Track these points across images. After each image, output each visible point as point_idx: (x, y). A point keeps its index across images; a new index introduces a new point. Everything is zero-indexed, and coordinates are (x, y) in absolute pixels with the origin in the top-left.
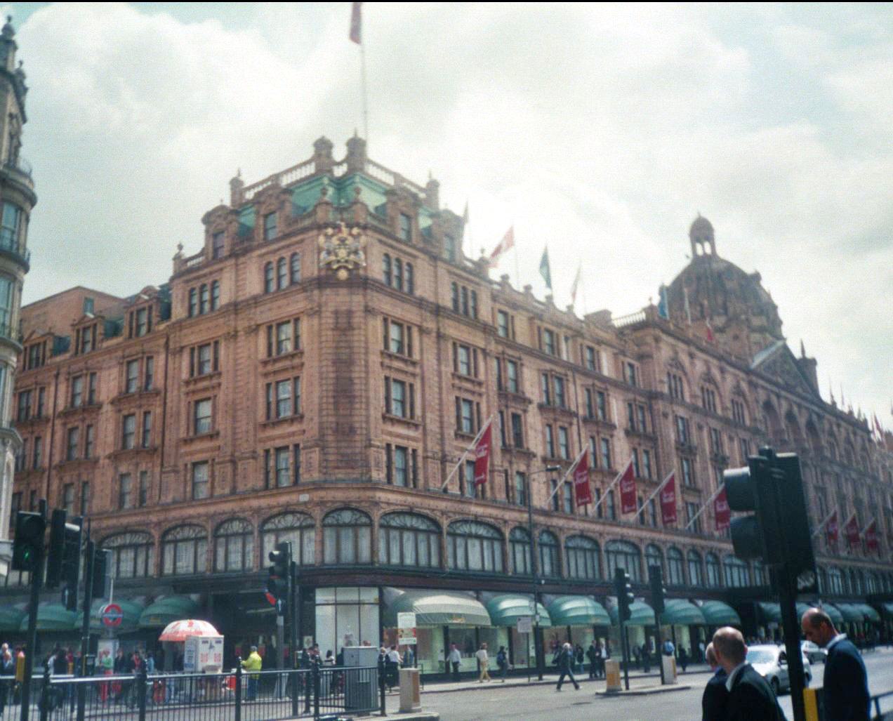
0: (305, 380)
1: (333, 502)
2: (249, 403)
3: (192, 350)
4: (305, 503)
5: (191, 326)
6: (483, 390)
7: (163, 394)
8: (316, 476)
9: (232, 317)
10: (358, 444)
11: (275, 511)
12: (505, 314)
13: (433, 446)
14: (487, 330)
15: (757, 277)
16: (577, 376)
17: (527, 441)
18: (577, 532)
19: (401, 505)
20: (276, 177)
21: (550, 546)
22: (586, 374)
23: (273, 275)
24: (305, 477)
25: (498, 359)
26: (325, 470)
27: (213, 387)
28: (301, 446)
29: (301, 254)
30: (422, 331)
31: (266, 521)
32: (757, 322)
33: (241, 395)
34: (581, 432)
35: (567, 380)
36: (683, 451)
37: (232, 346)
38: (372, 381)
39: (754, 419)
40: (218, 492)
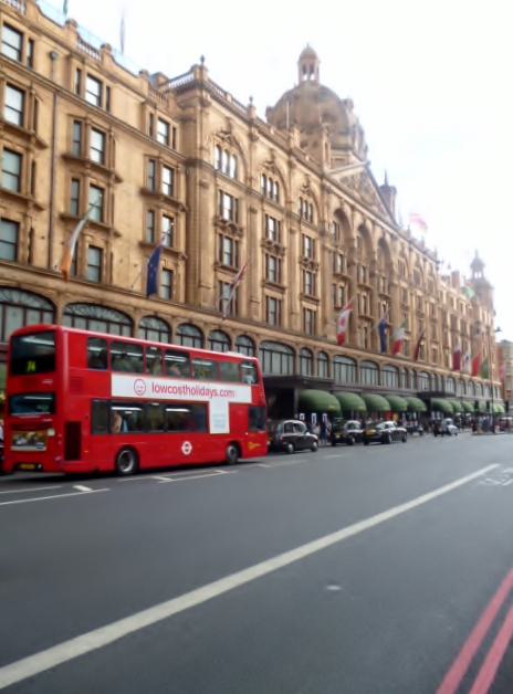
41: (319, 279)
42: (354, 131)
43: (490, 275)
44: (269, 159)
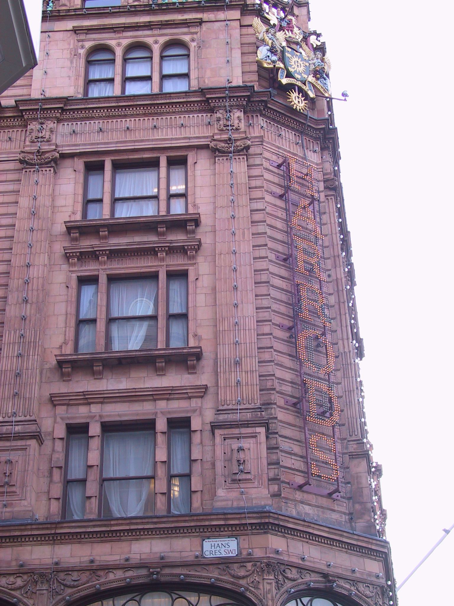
0: (205, 282)
1: (300, 569)
2: (28, 310)
28: (195, 424)
29: (193, 45)
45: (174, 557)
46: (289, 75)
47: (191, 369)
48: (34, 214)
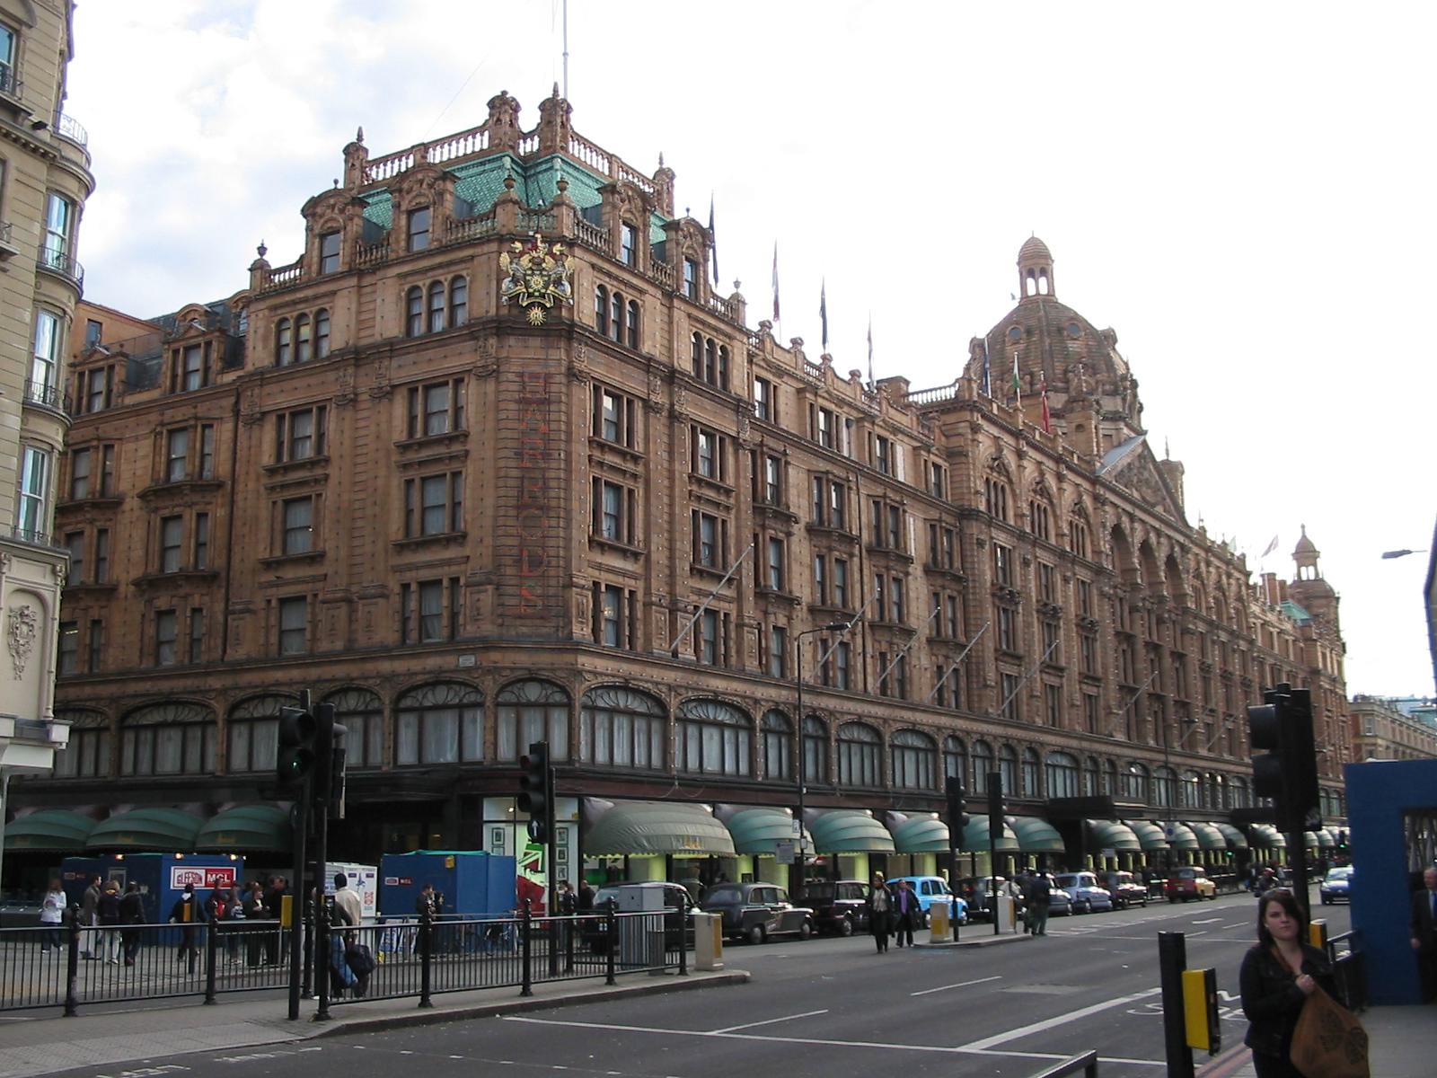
0: (470, 479)
1: (512, 669)
3: (281, 418)
4: (468, 670)
5: (279, 379)
6: (732, 501)
7: (229, 487)
8: (488, 629)
9: (351, 370)
10: (553, 582)
11: (419, 679)
12: (765, 383)
13: (659, 588)
14: (740, 407)
15: (1109, 338)
16: (861, 481)
17: (790, 580)
18: (855, 718)
19: (613, 676)
20: (424, 148)
21: (815, 738)
22: (874, 479)
23: (420, 307)
24: (468, 630)
25: (753, 453)
26: (500, 621)
27: (316, 481)
28: (462, 581)
29: (468, 279)
30: (648, 407)
31: (403, 695)
32: (1110, 404)
33: (363, 495)
34: (864, 566)
35: (850, 488)
36: (1001, 598)
37: (348, 414)
38: (575, 485)
39: (1097, 553)
40: (324, 646)
41: (1098, 644)
42: (1124, 387)
43: (1331, 571)
44: (1038, 479)
45: (446, 667)
46: (530, 295)
47: (462, 545)
48: (378, 437)
